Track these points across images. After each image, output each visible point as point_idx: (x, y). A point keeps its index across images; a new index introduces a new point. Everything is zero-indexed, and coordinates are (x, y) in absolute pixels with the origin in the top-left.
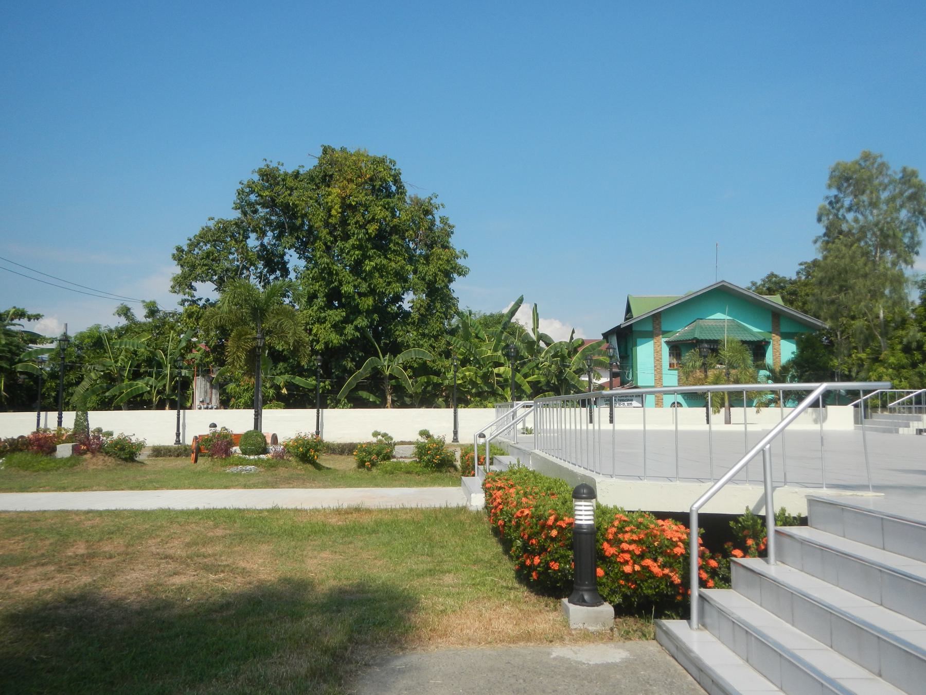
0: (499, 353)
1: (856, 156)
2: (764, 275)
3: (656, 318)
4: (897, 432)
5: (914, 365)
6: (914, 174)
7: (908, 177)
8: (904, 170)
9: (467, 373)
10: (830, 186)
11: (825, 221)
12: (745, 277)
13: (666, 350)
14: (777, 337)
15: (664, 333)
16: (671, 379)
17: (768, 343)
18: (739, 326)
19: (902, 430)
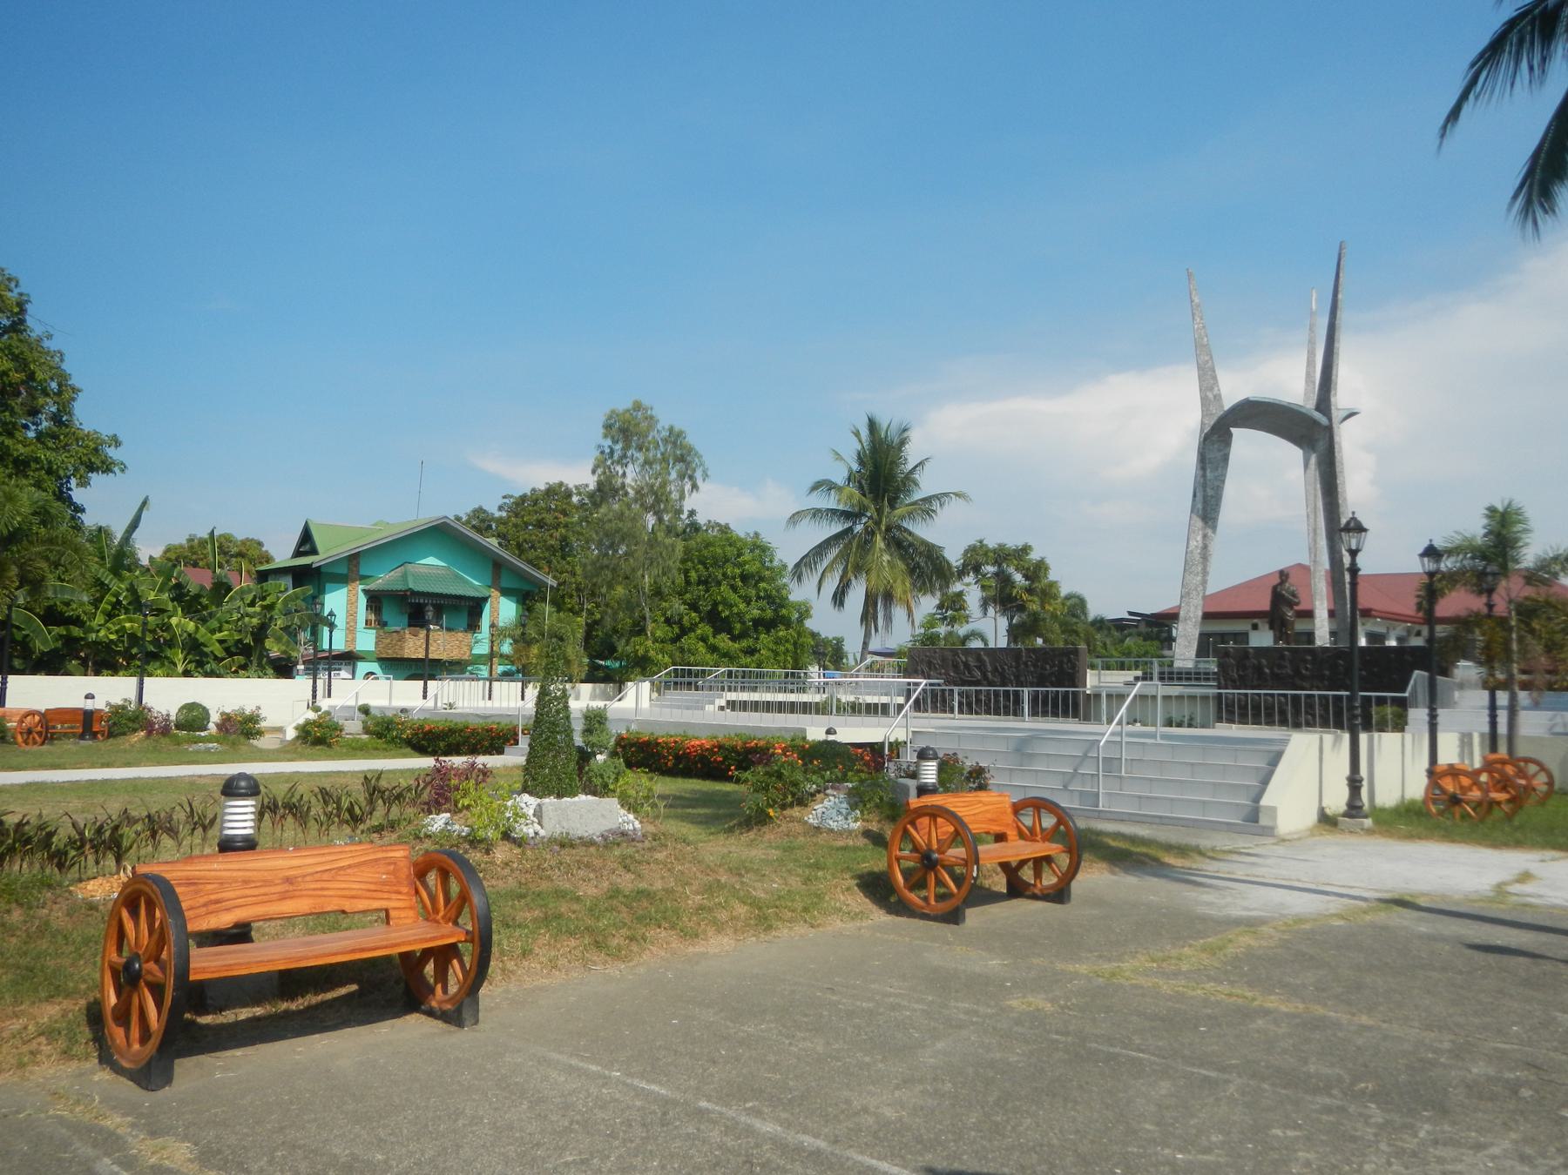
0: (166, 596)
1: (629, 405)
2: (469, 509)
3: (354, 559)
4: (703, 708)
5: (675, 640)
6: (680, 434)
7: (675, 437)
8: (671, 430)
9: (128, 625)
10: (605, 436)
11: (600, 471)
12: (454, 505)
13: (362, 601)
14: (495, 593)
15: (363, 578)
16: (366, 641)
17: (485, 599)
18: (457, 577)
19: (709, 708)
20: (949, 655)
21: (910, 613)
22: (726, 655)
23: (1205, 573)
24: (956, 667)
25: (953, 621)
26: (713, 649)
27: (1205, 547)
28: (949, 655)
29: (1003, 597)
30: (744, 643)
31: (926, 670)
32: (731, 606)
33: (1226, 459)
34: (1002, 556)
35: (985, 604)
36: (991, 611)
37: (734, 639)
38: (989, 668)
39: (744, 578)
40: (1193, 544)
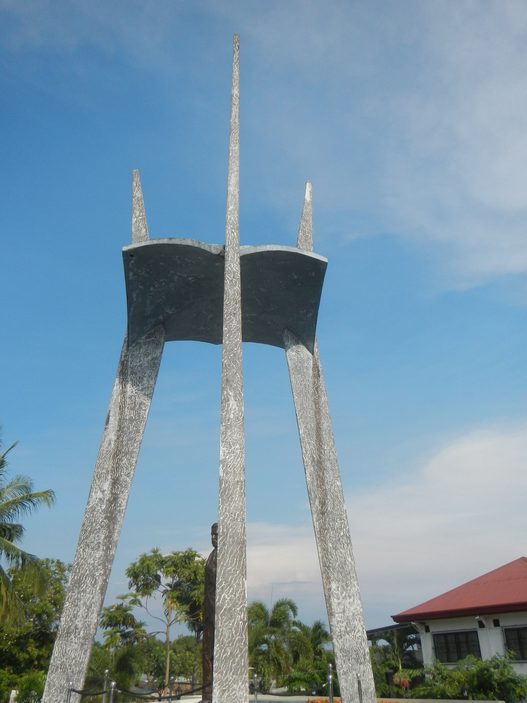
23: (109, 543)
27: (114, 499)
33: (155, 364)
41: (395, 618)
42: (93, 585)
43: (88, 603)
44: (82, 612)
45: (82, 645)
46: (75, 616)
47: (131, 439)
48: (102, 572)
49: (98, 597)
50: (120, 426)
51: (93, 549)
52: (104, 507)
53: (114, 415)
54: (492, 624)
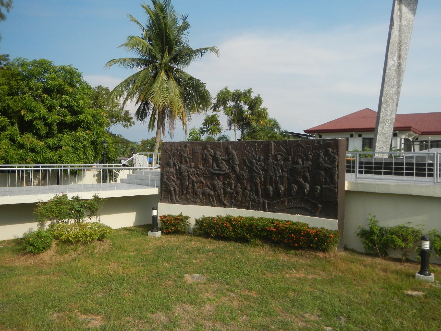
20: (199, 150)
21: (184, 124)
22: (33, 150)
23: (399, 85)
24: (205, 160)
25: (212, 132)
26: (21, 146)
27: (399, 65)
28: (199, 150)
29: (239, 119)
30: (50, 141)
31: (177, 163)
32: (31, 111)
34: (237, 96)
35: (230, 123)
36: (233, 127)
37: (40, 137)
38: (237, 162)
39: (48, 91)
40: (390, 63)
41: (306, 131)
42: (393, 102)
43: (391, 110)
44: (389, 113)
45: (390, 126)
46: (386, 114)
47: (406, 36)
48: (396, 97)
49: (395, 108)
50: (400, 28)
51: (391, 87)
52: (395, 68)
53: (396, 22)
54: (358, 136)
